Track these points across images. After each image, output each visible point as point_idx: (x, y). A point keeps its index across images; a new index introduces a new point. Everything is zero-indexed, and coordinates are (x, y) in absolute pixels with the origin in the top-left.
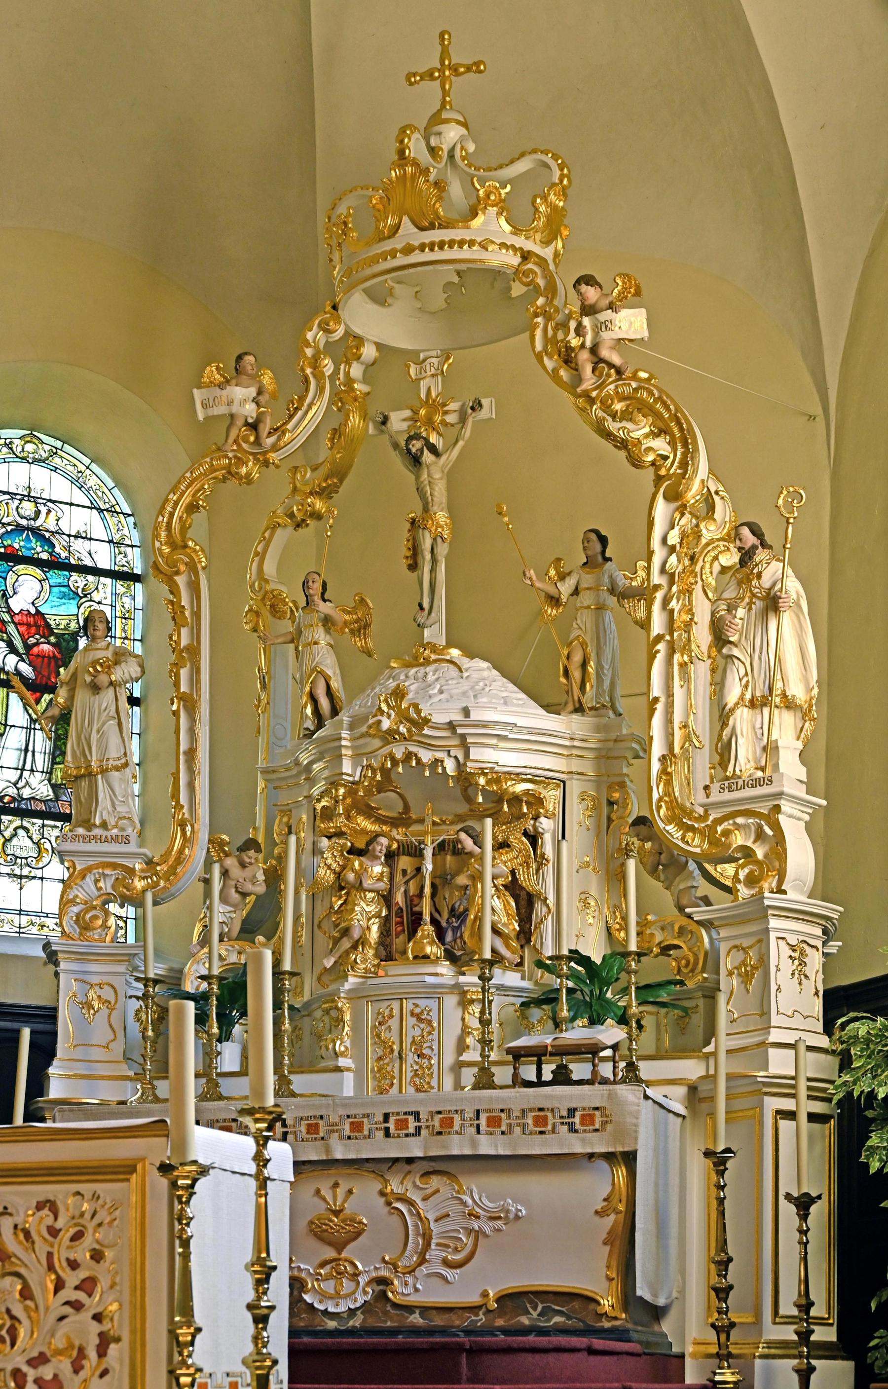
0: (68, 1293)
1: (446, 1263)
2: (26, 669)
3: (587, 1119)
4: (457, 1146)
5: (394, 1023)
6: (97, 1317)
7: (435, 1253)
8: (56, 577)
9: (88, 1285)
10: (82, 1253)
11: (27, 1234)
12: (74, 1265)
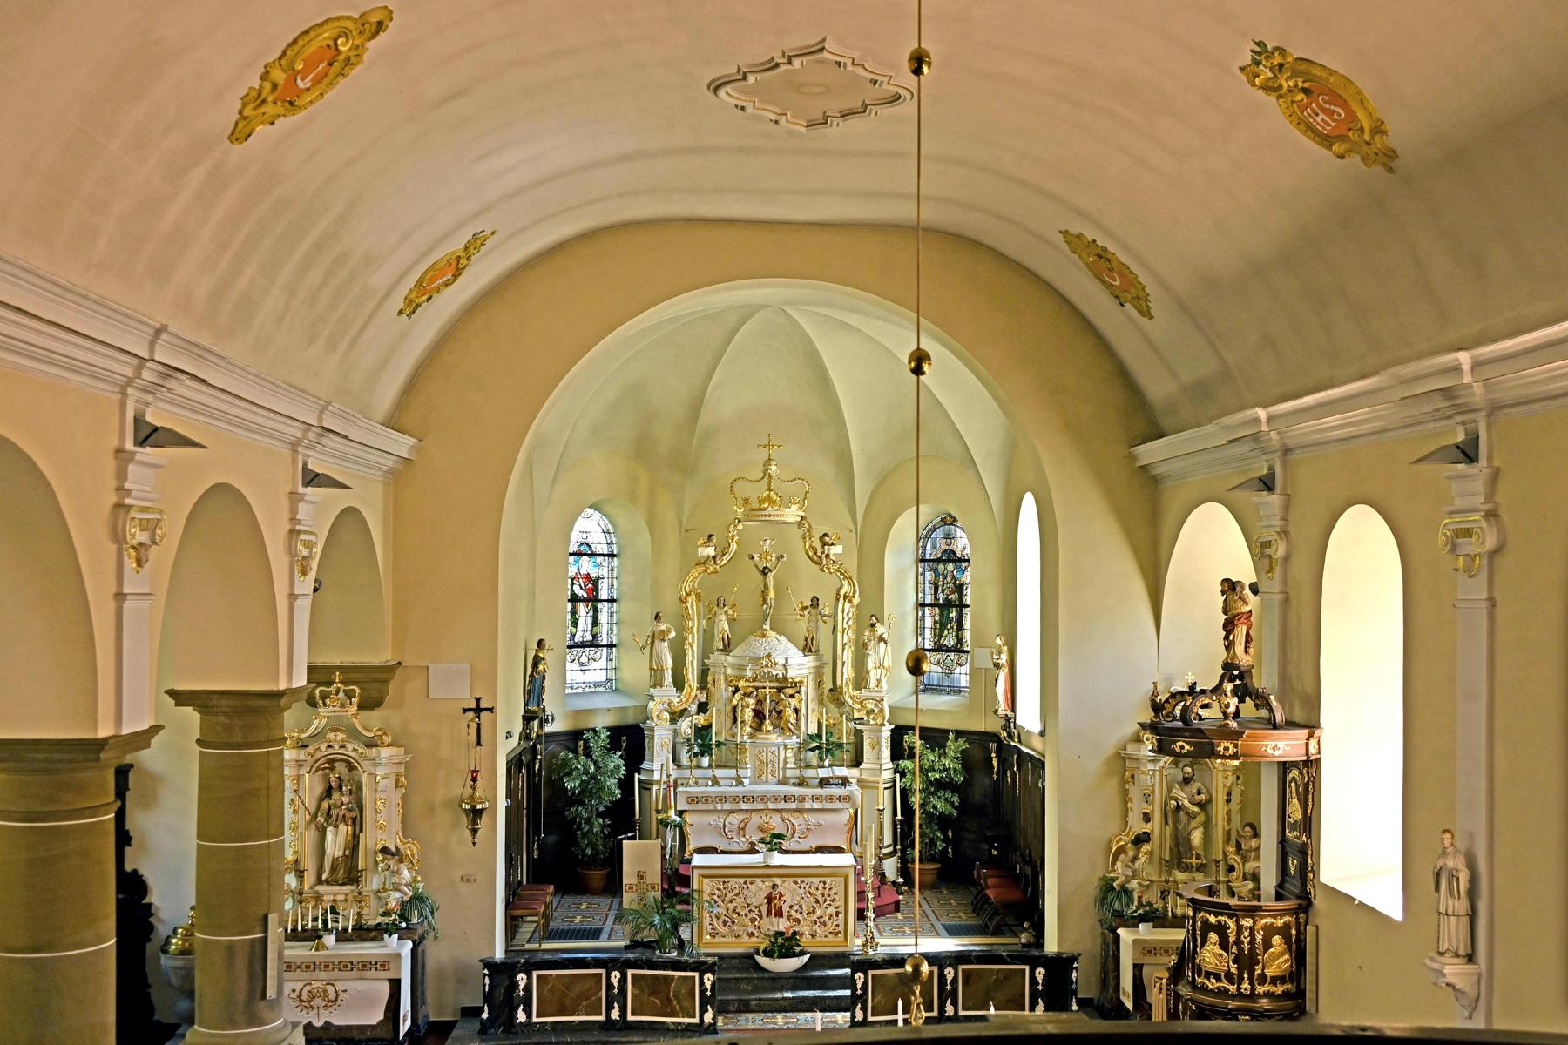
0: (828, 902)
1: (799, 837)
2: (585, 595)
3: (845, 799)
4: (807, 805)
5: (764, 754)
6: (835, 908)
7: (796, 835)
8: (593, 559)
10: (832, 892)
11: (817, 889)
12: (829, 895)
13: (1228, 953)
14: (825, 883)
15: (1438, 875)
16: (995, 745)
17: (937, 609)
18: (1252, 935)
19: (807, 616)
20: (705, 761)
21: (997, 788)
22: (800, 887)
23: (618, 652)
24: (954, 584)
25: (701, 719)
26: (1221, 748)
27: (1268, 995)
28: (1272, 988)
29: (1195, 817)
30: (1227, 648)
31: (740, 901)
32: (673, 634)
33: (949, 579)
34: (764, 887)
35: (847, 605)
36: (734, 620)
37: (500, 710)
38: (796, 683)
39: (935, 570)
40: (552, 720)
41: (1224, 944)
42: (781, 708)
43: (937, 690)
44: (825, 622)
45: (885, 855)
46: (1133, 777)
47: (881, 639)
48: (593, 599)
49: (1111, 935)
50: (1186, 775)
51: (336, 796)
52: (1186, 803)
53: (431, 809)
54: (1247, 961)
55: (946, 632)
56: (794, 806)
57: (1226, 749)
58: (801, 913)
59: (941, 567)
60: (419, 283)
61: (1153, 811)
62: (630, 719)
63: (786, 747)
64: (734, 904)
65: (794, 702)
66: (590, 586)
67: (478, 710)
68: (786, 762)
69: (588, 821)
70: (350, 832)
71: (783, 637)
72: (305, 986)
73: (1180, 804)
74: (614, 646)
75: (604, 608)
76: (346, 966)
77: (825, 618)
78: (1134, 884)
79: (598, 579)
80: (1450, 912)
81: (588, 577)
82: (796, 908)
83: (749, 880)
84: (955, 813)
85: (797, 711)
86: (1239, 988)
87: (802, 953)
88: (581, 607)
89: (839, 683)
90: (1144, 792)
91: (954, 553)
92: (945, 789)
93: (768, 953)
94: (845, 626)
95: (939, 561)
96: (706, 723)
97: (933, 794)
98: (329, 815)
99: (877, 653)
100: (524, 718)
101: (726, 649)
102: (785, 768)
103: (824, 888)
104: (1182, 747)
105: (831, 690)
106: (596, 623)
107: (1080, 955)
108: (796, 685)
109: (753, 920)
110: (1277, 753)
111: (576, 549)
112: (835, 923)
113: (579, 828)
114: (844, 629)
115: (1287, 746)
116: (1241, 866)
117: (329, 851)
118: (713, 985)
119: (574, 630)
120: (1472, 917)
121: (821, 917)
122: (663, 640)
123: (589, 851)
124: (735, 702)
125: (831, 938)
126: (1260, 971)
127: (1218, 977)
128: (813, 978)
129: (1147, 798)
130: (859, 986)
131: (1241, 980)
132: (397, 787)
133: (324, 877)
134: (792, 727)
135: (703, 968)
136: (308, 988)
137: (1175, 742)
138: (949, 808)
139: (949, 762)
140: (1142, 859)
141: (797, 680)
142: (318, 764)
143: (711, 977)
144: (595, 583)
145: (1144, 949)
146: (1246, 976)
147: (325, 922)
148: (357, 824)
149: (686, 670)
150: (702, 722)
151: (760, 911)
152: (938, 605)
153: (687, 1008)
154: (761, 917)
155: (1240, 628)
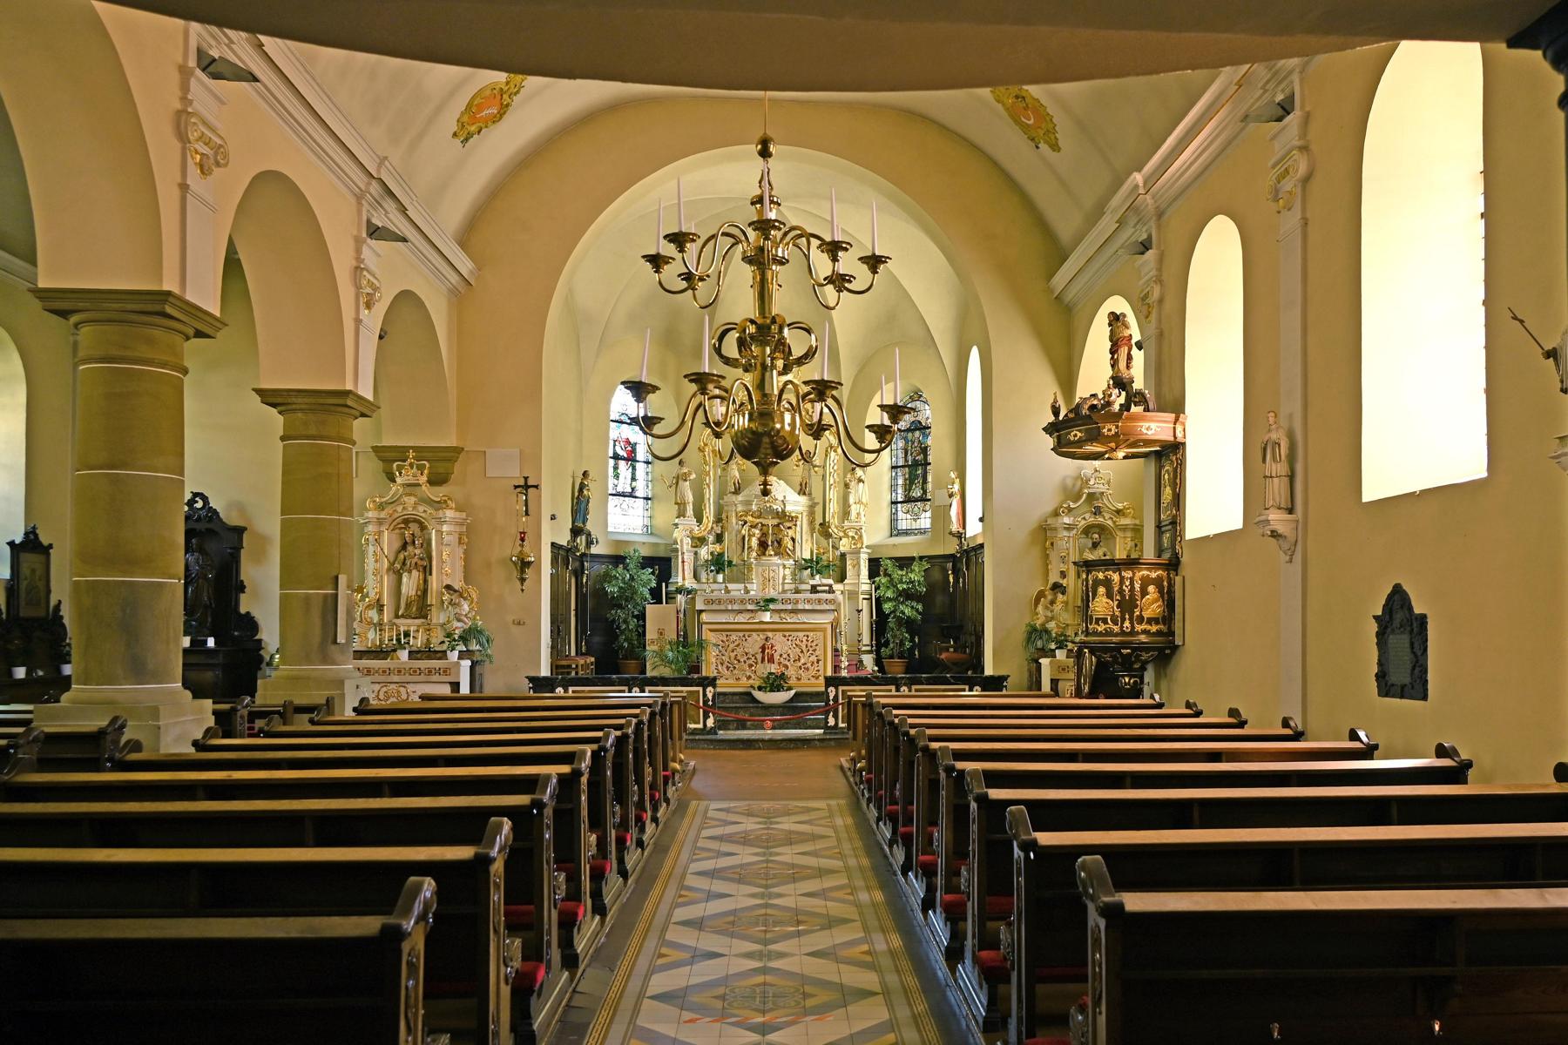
0: (810, 652)
2: (626, 455)
4: (800, 607)
5: (767, 572)
9: (814, 650)
13: (1113, 601)
14: (808, 636)
15: (1265, 450)
16: (951, 564)
17: (907, 469)
18: (1132, 584)
19: (802, 466)
20: (720, 577)
21: (952, 596)
22: (788, 640)
23: (652, 503)
24: (920, 447)
25: (717, 548)
26: (1105, 430)
27: (1145, 632)
28: (1148, 627)
30: (1113, 366)
31: (739, 651)
32: (693, 476)
33: (916, 444)
34: (759, 639)
35: (833, 454)
36: (744, 470)
37: (543, 487)
38: (792, 517)
39: (905, 439)
40: (597, 542)
41: (1109, 595)
42: (781, 536)
43: (906, 533)
44: (816, 472)
45: (864, 651)
46: (1052, 544)
47: (860, 480)
48: (631, 459)
51: (410, 548)
53: (489, 565)
54: (1127, 605)
55: (914, 487)
56: (790, 607)
57: (1110, 430)
58: (789, 661)
59: (910, 434)
60: (469, 106)
61: (1068, 568)
62: (662, 554)
63: (784, 567)
64: (735, 653)
65: (791, 533)
66: (629, 448)
67: (527, 487)
68: (784, 579)
69: (625, 621)
70: (421, 578)
71: (782, 482)
72: (382, 687)
74: (650, 499)
75: (640, 467)
76: (415, 671)
77: (816, 469)
78: (1052, 625)
79: (636, 444)
80: (1274, 475)
81: (628, 442)
82: (785, 656)
83: (747, 634)
84: (919, 617)
85: (793, 540)
86: (1122, 627)
87: (790, 689)
88: (622, 464)
89: (827, 520)
91: (920, 422)
92: (912, 600)
93: (760, 688)
94: (832, 470)
95: (908, 430)
96: (721, 551)
97: (902, 603)
98: (404, 563)
99: (857, 491)
100: (572, 530)
101: (737, 491)
102: (783, 584)
103: (807, 641)
104: (1075, 435)
105: (821, 524)
106: (633, 479)
107: (1009, 676)
108: (793, 519)
109: (751, 666)
110: (1149, 433)
111: (617, 418)
112: (816, 669)
113: (618, 627)
114: (830, 473)
115: (1158, 427)
117: (404, 589)
118: (714, 696)
119: (616, 482)
120: (1292, 477)
121: (805, 664)
122: (686, 480)
123: (626, 645)
124: (743, 532)
125: (813, 681)
126: (1138, 613)
127: (1105, 621)
128: (796, 707)
129: (1063, 559)
130: (831, 698)
131: (1123, 620)
132: (460, 543)
133: (400, 614)
134: (789, 552)
135: (706, 682)
136: (385, 689)
137: (1069, 433)
138: (915, 613)
139: (916, 574)
140: (1058, 607)
141: (793, 515)
142: (395, 523)
143: (712, 690)
144: (634, 446)
146: (1127, 616)
147: (399, 640)
148: (427, 570)
149: (705, 505)
150: (718, 550)
151: (756, 658)
152: (908, 466)
153: (693, 716)
154: (756, 663)
155: (1122, 349)
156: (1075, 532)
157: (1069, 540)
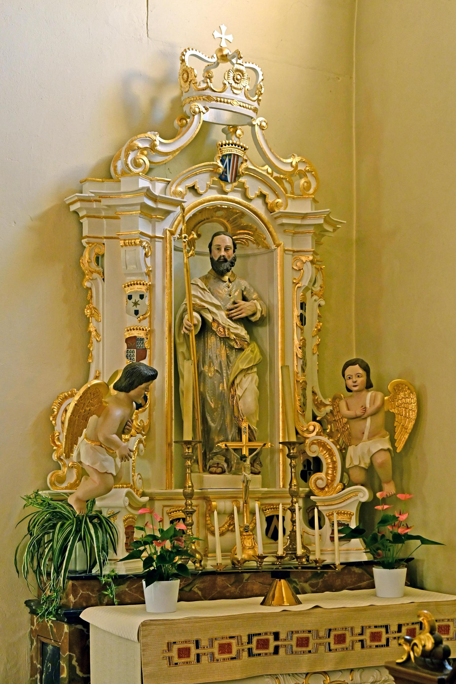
29: (241, 350)
46: (98, 259)
49: (66, 628)
50: (223, 253)
52: (222, 316)
61: (150, 333)
73: (209, 317)
90: (129, 291)
116: (338, 458)
145: (169, 646)
156: (166, 224)
157: (152, 248)
